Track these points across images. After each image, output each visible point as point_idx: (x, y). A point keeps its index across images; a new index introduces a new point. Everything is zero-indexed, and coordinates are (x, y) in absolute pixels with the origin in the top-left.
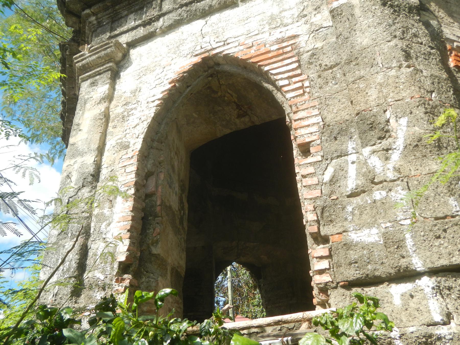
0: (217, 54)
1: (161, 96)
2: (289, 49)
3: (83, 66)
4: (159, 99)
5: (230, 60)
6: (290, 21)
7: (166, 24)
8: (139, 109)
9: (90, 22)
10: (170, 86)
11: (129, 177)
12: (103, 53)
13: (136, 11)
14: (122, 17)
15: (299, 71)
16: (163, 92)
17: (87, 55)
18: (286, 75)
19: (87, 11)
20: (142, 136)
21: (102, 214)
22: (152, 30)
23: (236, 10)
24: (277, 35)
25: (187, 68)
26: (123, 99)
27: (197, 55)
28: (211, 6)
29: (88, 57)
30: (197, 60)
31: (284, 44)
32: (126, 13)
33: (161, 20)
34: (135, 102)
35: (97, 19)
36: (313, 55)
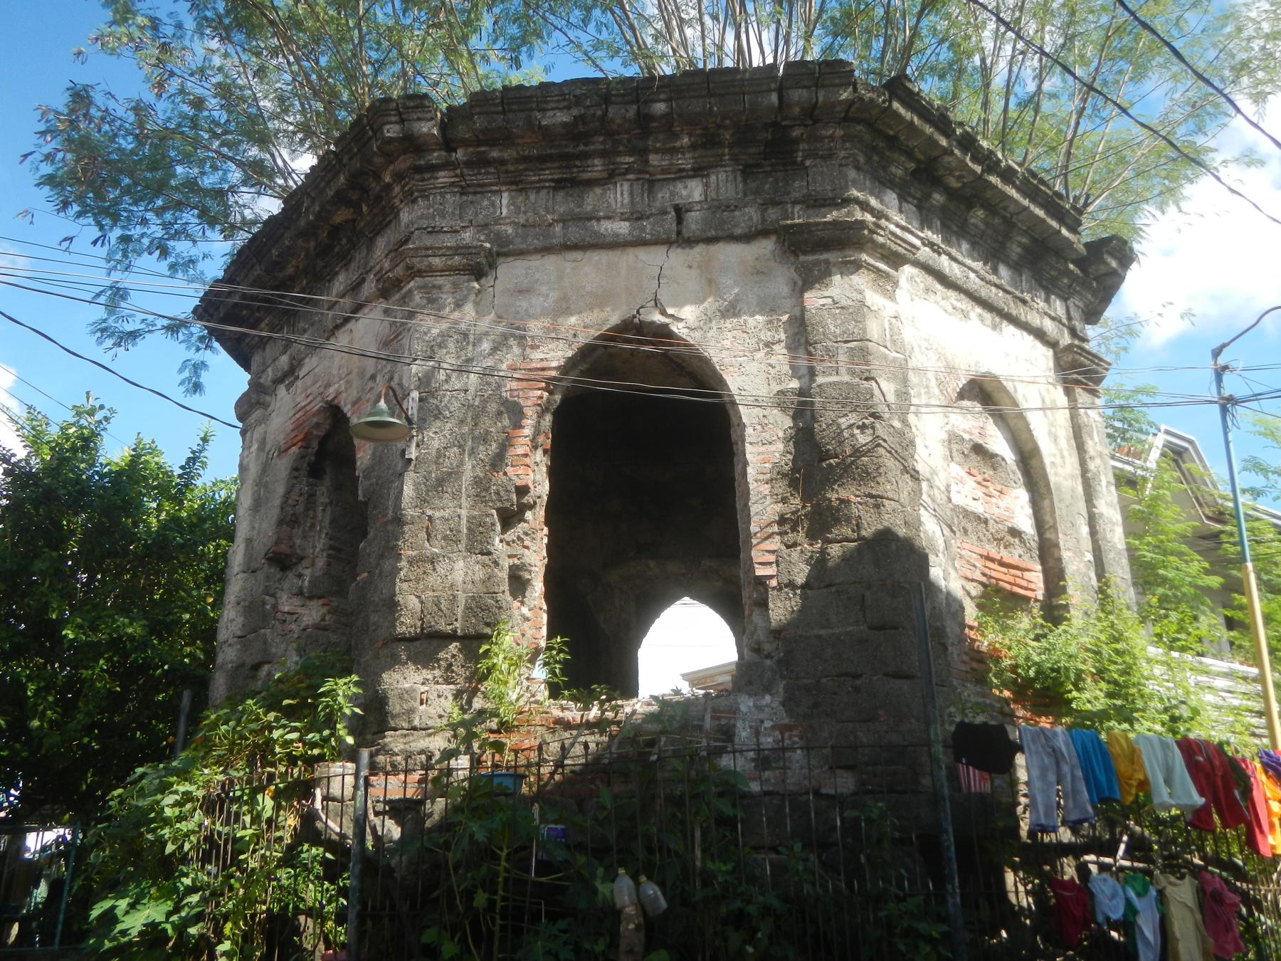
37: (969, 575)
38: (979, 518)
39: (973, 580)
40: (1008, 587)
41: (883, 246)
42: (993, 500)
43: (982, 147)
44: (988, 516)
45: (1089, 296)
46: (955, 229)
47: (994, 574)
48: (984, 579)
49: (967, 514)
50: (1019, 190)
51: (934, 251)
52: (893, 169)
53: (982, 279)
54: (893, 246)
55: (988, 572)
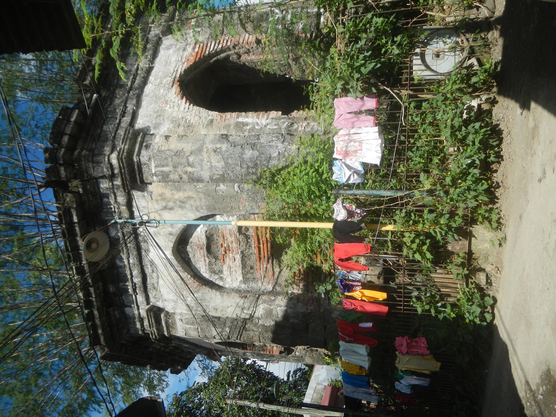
0: (180, 75)
1: (188, 104)
2: (202, 45)
3: (127, 153)
4: (190, 105)
5: (187, 71)
6: (185, 44)
7: (134, 102)
8: (189, 117)
9: (85, 156)
10: (184, 99)
11: (233, 116)
12: (129, 135)
13: (104, 124)
14: (100, 134)
15: (218, 41)
16: (186, 103)
17: (123, 147)
18: (217, 45)
19: (76, 153)
20: (210, 112)
21: (250, 129)
22: (131, 111)
23: (155, 68)
24: (189, 49)
25: (178, 89)
26: (173, 129)
27: (172, 87)
28: (143, 77)
29: (124, 147)
30: (176, 86)
31: (198, 46)
32: (99, 130)
33: (128, 105)
34: (181, 120)
35: (87, 151)
36: (212, 37)
37: (271, 273)
38: (242, 257)
39: (273, 269)
40: (269, 245)
41: (157, 329)
42: (231, 246)
43: (83, 295)
44: (240, 252)
45: (83, 163)
46: (115, 271)
47: (266, 255)
48: (270, 261)
49: (244, 266)
50: (81, 261)
51: (136, 287)
52: (118, 316)
53: (129, 254)
54: (154, 325)
55: (266, 258)
